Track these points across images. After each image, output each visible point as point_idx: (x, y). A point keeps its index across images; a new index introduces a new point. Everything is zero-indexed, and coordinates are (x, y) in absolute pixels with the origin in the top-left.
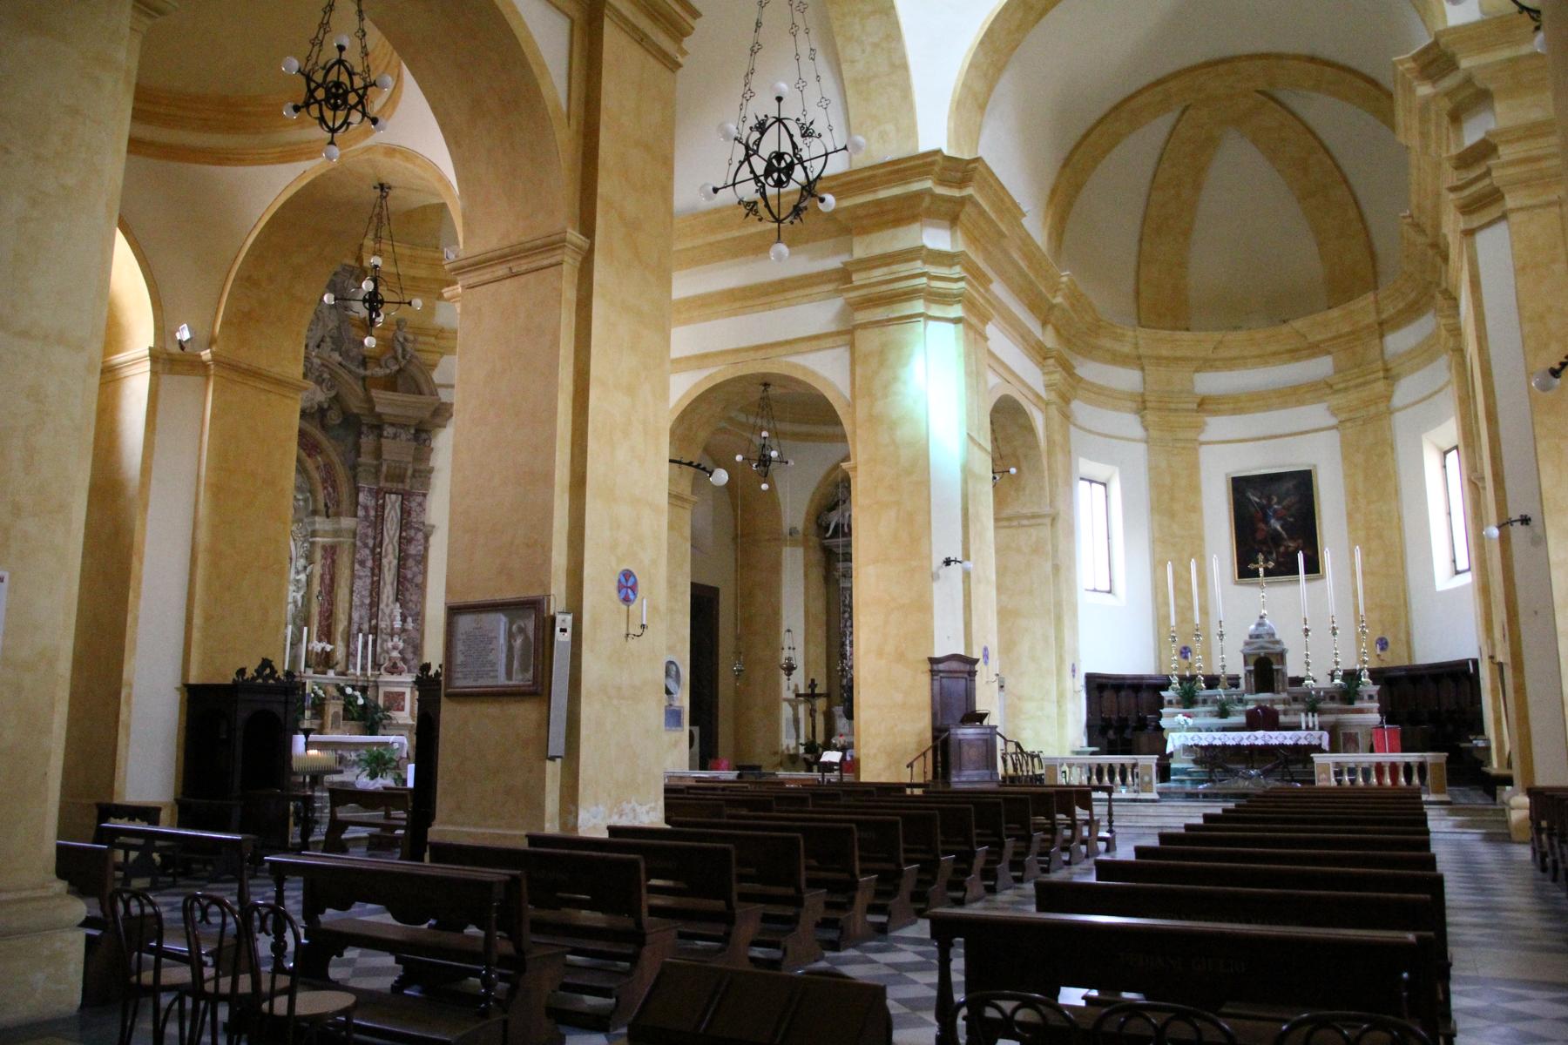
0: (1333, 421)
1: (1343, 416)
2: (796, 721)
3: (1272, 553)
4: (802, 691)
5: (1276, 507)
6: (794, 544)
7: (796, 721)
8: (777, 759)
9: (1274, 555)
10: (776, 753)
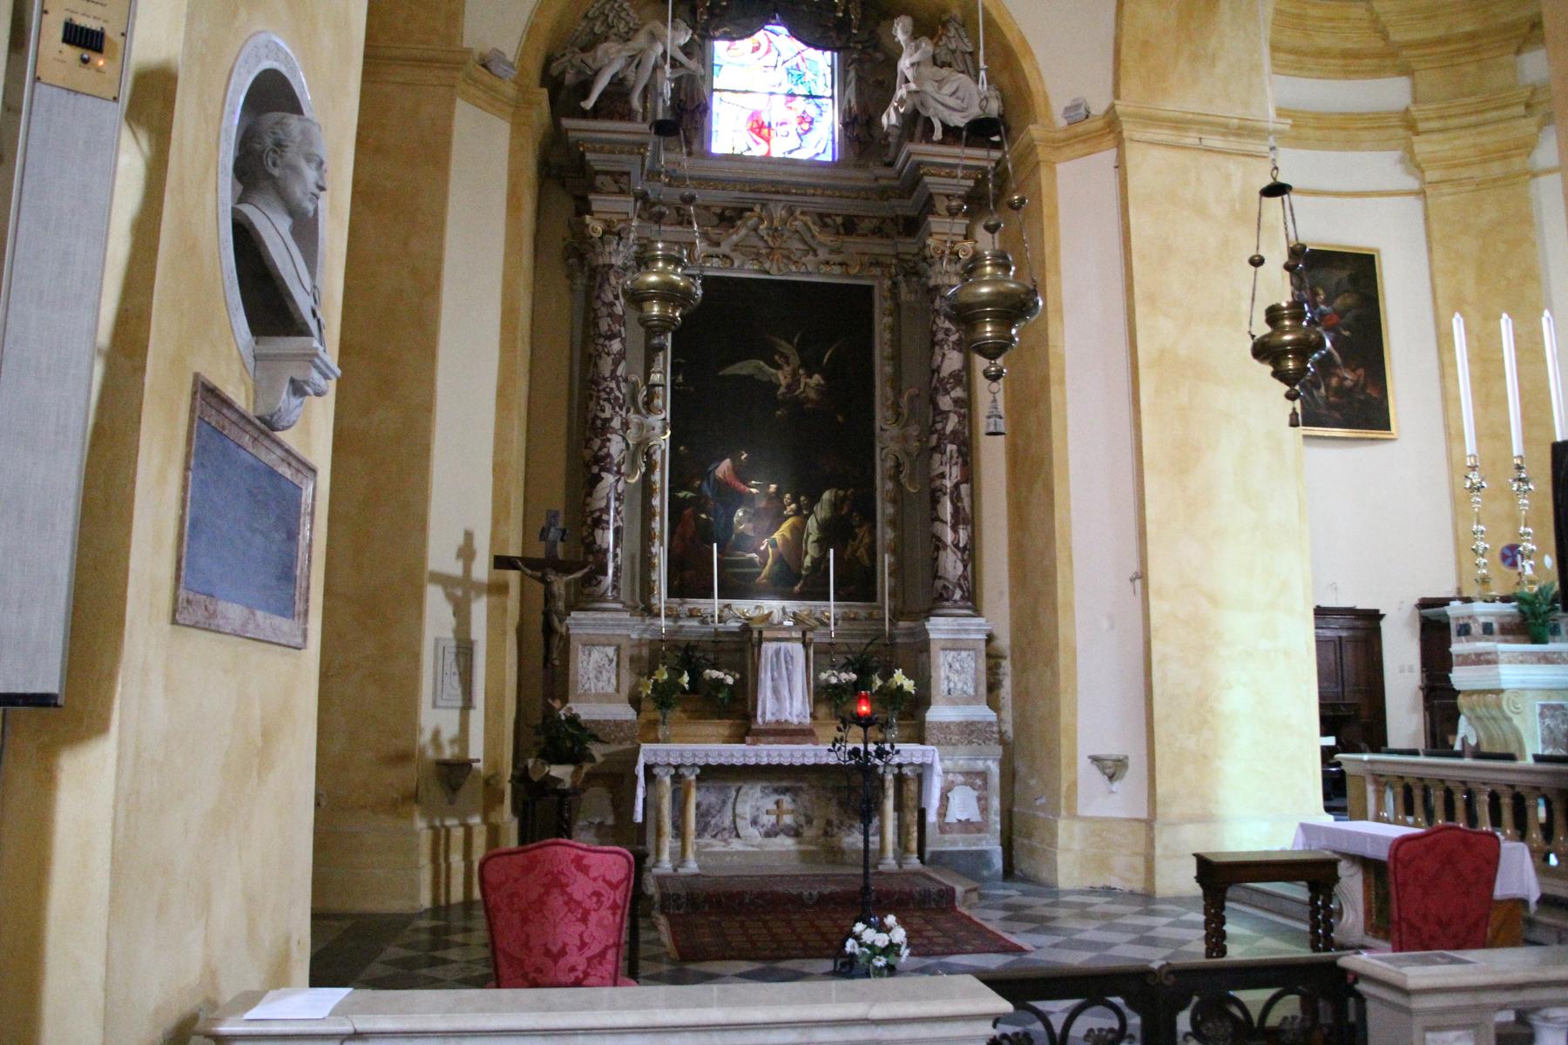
0: (1412, 183)
1: (1431, 176)
2: (465, 650)
3: (1318, 388)
4: (514, 551)
5: (1323, 307)
6: (491, 101)
7: (465, 650)
8: (408, 776)
9: (1323, 390)
10: (403, 757)
